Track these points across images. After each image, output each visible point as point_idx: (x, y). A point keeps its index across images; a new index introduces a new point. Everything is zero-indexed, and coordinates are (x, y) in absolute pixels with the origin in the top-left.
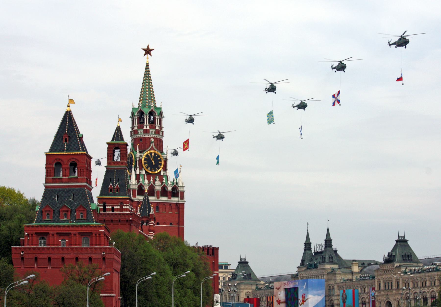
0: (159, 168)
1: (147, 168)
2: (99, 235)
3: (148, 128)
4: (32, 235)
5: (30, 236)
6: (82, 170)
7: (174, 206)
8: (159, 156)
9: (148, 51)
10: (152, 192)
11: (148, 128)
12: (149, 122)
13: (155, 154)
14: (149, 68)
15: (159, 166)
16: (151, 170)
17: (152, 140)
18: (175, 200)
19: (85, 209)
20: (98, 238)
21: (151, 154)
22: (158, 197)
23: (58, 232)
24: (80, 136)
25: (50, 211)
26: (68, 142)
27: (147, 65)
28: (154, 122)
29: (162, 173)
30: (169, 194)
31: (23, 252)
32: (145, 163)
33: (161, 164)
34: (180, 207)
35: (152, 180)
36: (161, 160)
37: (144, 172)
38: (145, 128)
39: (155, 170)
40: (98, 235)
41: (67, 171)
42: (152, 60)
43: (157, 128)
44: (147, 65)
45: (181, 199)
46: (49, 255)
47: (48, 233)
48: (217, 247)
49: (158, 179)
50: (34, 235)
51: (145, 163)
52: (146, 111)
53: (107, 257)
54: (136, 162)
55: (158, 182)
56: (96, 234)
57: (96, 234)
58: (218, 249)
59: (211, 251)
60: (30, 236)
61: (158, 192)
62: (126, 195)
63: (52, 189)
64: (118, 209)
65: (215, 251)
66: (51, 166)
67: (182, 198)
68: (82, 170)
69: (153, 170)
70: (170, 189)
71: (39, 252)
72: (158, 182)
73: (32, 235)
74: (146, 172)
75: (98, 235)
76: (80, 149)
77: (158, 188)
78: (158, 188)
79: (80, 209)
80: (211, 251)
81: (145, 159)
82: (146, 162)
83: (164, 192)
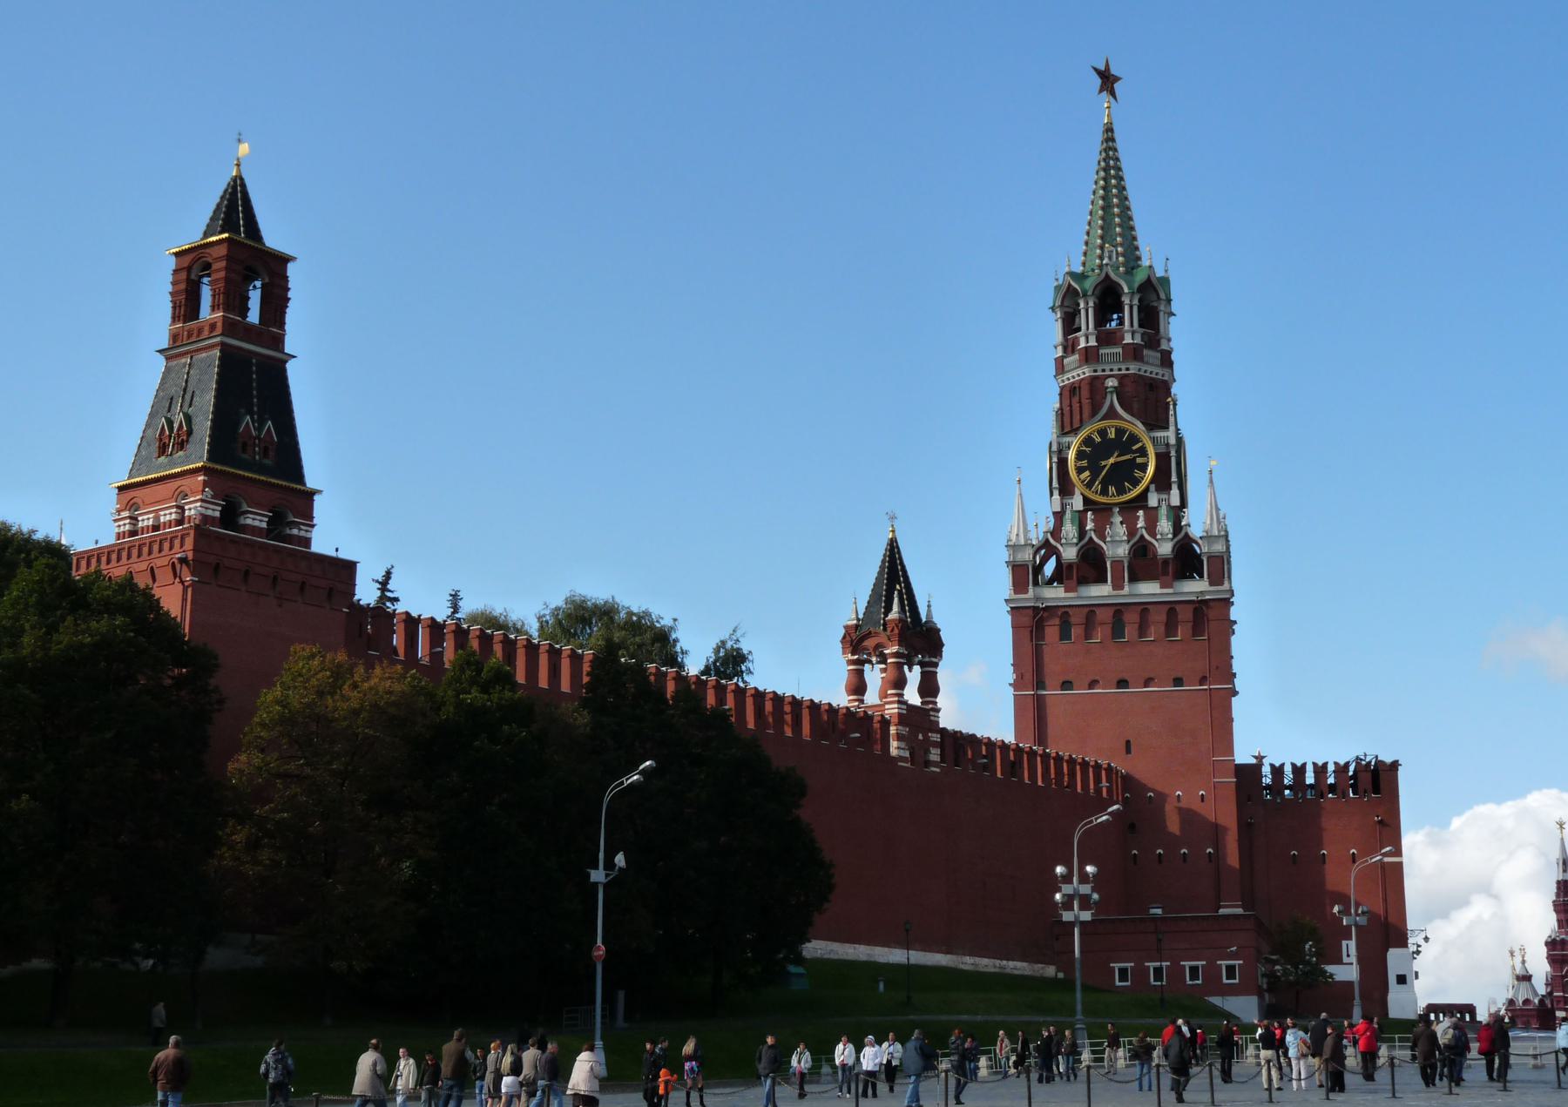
3: (1093, 342)
9: (1108, 80)
10: (1091, 565)
14: (1113, 140)
15: (1138, 474)
22: (1118, 585)
27: (1109, 129)
32: (1080, 470)
34: (1211, 620)
42: (1126, 112)
44: (1109, 129)
45: (1211, 584)
48: (1388, 758)
49: (1117, 519)
55: (1118, 529)
58: (1395, 765)
61: (1117, 563)
64: (261, 529)
65: (1382, 776)
69: (1112, 489)
72: (1118, 529)
74: (1086, 501)
77: (1117, 547)
78: (1117, 547)
81: (1080, 455)
82: (1084, 463)
83: (1142, 562)
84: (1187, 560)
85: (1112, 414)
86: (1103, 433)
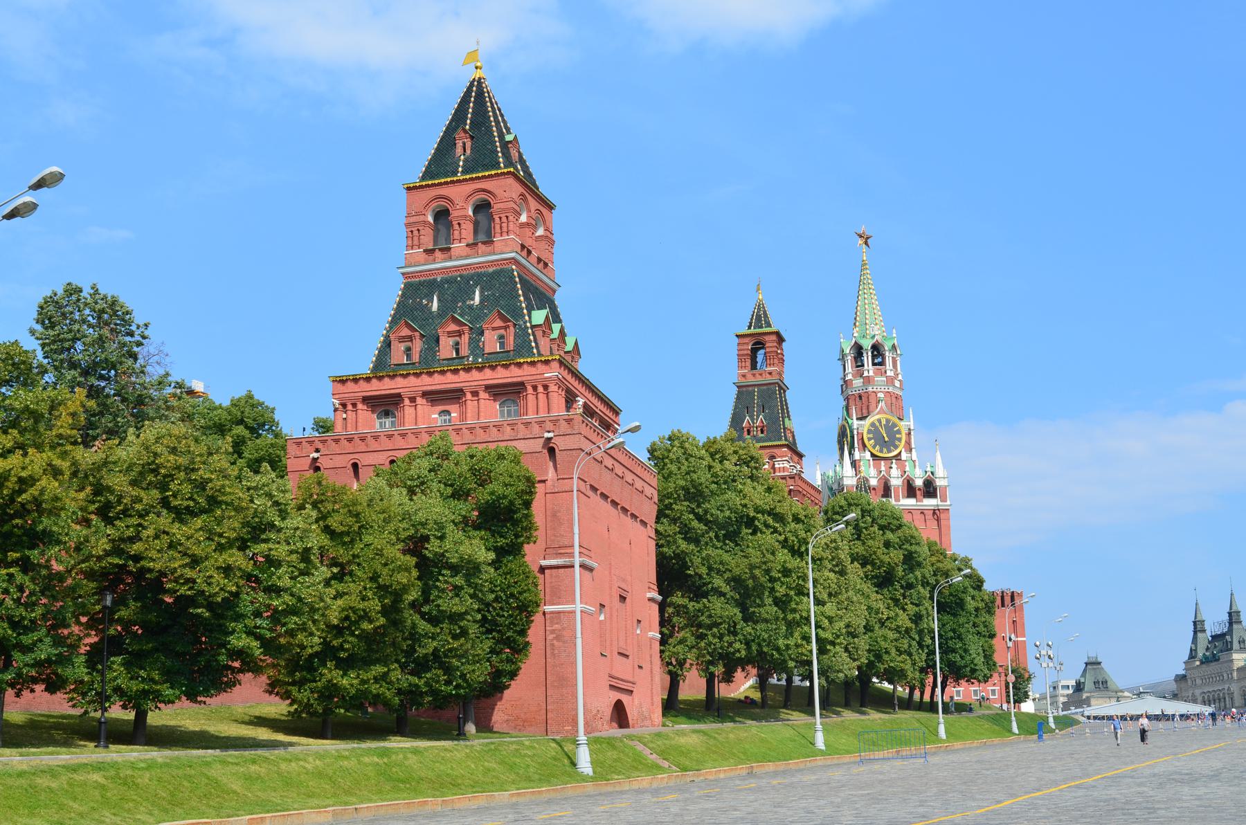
0: (896, 447)
1: (874, 447)
2: (546, 387)
3: (871, 373)
4: (354, 405)
5: (350, 407)
6: (504, 219)
7: (929, 515)
8: (895, 425)
11: (871, 373)
12: (874, 364)
13: (888, 421)
16: (881, 451)
17: (881, 395)
18: (930, 503)
19: (507, 320)
20: (540, 396)
21: (879, 421)
23: (425, 388)
24: (509, 138)
25: (410, 339)
26: (468, 152)
28: (882, 363)
29: (904, 456)
30: (918, 493)
31: (317, 451)
32: (869, 439)
33: (900, 440)
35: (883, 468)
36: (899, 432)
37: (868, 455)
38: (866, 374)
39: (889, 451)
40: (540, 389)
41: (463, 226)
43: (889, 373)
46: (391, 453)
47: (399, 395)
50: (360, 406)
51: (869, 439)
52: (867, 344)
53: (559, 444)
54: (852, 437)
55: (895, 472)
56: (535, 388)
57: (535, 388)
59: (1007, 599)
60: (350, 407)
61: (897, 488)
62: (780, 439)
63: (422, 279)
66: (421, 218)
67: (944, 500)
68: (504, 219)
70: (919, 483)
71: (362, 448)
72: (895, 472)
73: (354, 405)
74: (873, 455)
75: (540, 389)
76: (499, 163)
78: (896, 482)
79: (495, 325)
80: (1007, 599)
81: (869, 432)
84: (930, 489)
85: (882, 411)
86: (879, 421)
